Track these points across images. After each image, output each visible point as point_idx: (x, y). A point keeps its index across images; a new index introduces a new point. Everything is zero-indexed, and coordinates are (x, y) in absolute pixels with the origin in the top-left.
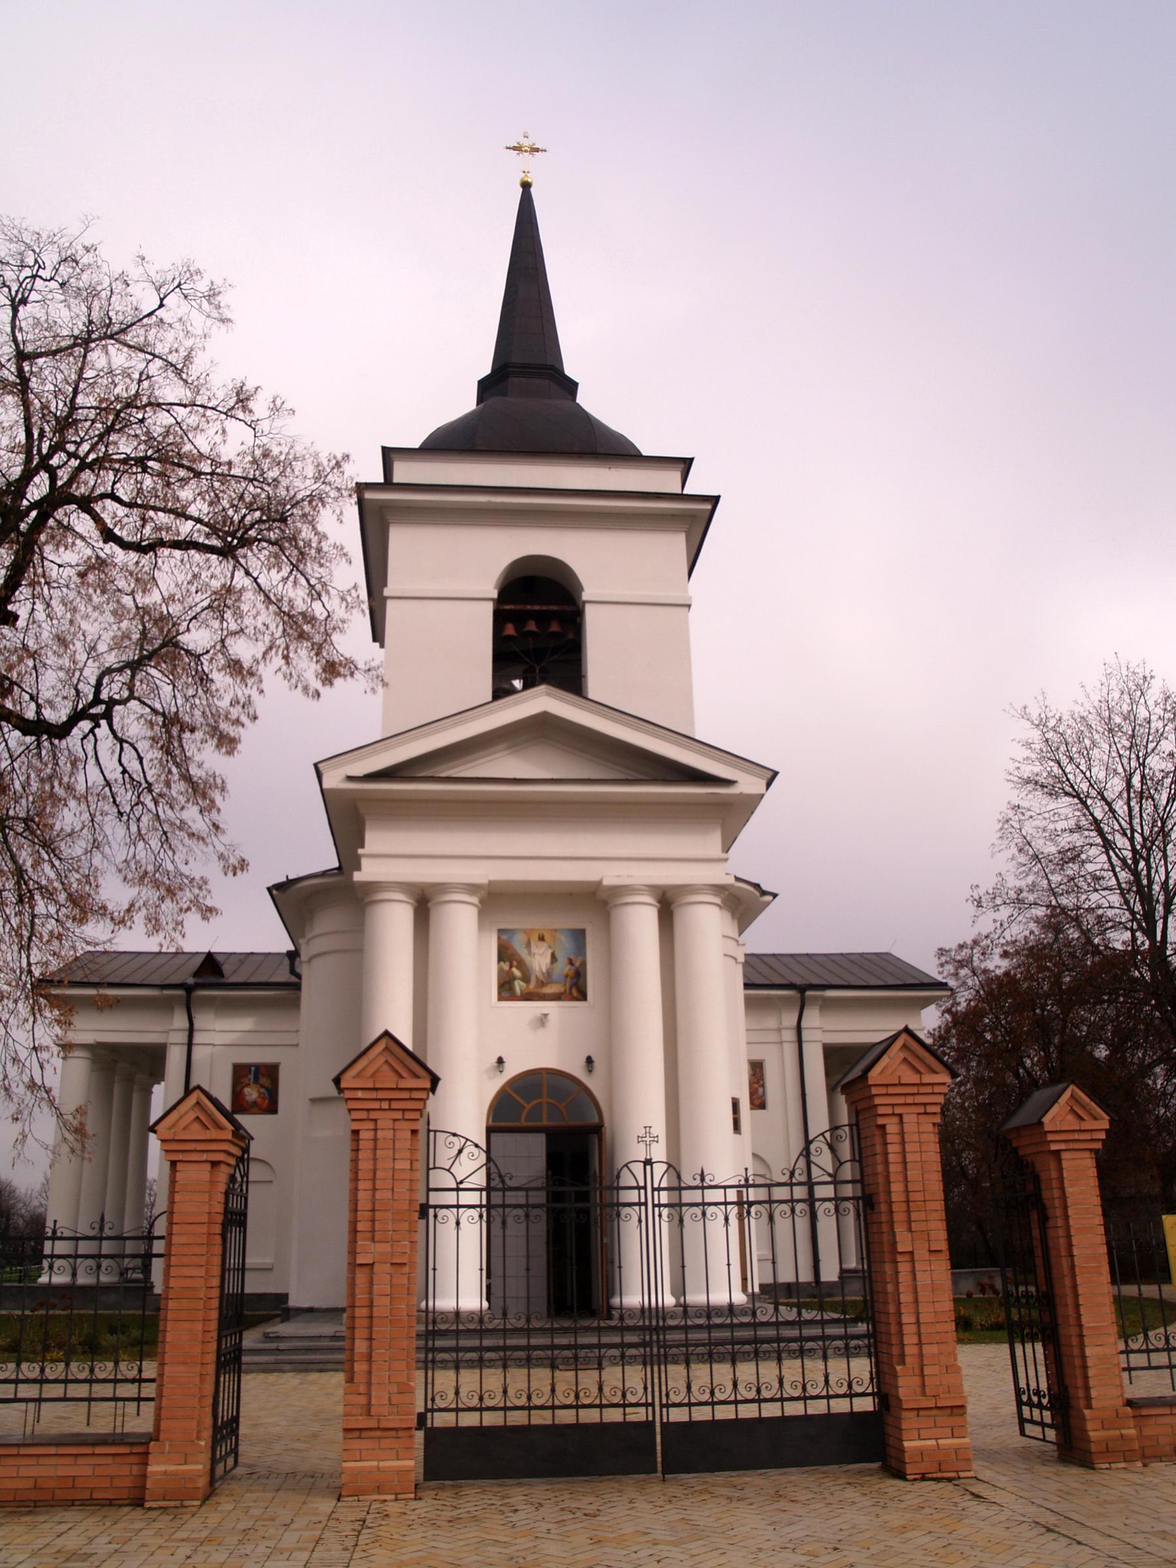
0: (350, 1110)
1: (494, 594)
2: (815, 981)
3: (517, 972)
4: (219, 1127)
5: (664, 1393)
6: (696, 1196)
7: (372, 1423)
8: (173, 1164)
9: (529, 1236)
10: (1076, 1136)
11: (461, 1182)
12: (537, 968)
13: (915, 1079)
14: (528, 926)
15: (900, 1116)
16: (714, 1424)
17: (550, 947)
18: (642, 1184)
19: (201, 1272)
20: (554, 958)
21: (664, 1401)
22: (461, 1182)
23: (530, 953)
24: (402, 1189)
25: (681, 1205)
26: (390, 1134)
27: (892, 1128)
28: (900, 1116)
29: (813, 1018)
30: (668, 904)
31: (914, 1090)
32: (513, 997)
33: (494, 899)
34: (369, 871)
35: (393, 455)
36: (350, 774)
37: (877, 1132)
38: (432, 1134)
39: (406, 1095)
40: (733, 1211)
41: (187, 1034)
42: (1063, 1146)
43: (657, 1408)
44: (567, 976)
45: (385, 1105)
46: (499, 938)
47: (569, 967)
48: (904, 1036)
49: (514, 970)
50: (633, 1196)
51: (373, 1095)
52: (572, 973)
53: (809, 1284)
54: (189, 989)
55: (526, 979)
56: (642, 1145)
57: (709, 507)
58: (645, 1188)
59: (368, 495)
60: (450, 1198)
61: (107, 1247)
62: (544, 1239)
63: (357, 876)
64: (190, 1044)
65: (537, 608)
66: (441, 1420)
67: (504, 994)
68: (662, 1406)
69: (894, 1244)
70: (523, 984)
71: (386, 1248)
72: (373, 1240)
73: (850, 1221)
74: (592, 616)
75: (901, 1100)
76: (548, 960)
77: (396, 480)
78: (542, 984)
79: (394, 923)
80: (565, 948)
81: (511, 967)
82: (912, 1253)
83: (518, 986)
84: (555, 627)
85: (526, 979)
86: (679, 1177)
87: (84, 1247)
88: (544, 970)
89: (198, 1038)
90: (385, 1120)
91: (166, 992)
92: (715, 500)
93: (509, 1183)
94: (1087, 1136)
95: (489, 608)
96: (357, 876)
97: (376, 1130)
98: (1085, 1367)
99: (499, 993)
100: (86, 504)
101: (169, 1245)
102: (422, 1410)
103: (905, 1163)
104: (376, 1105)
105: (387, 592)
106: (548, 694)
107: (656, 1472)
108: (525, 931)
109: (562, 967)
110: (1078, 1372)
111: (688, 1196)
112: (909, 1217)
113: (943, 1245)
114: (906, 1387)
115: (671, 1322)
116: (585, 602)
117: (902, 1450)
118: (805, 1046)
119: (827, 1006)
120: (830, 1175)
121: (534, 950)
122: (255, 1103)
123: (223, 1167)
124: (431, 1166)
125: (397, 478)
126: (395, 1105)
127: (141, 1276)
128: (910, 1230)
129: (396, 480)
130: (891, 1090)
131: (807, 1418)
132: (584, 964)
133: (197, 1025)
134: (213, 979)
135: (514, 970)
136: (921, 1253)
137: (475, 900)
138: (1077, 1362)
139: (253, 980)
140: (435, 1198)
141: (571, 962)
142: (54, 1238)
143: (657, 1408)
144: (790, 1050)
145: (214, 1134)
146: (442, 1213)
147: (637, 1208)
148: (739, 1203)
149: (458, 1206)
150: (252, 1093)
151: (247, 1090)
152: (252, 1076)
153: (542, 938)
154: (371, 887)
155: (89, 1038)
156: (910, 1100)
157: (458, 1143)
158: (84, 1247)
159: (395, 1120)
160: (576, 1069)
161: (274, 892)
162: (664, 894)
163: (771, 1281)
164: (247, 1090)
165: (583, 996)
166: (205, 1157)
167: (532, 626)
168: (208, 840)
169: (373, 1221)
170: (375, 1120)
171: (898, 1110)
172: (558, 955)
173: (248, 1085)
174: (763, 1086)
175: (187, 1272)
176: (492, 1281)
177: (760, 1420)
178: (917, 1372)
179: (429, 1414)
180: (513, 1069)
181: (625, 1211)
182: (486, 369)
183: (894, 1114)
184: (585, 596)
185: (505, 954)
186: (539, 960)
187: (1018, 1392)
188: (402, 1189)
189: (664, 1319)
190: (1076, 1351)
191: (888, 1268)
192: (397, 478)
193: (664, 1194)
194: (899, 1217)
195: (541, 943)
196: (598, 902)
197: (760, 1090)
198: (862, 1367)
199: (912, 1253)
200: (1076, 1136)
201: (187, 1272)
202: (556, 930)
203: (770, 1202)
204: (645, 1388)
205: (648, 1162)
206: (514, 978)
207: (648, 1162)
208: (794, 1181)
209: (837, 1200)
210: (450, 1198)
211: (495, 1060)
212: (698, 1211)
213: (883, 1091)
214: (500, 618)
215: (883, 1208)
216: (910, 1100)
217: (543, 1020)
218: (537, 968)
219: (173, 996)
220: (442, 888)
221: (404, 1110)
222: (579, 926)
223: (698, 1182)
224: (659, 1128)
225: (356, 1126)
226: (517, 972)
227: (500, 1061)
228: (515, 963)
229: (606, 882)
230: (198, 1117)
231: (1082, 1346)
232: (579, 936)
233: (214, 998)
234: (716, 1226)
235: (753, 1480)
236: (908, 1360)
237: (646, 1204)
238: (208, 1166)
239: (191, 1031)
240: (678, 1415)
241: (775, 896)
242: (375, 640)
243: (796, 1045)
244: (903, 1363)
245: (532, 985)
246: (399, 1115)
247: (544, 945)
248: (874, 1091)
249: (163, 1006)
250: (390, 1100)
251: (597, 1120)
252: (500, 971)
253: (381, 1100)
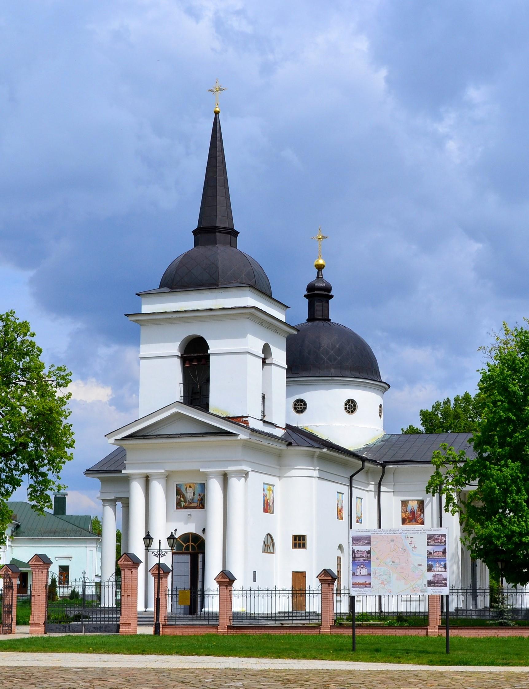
3: (182, 499)
14: (187, 482)
32: (181, 508)
55: (185, 502)
61: (244, 592)
65: (195, 355)
74: (213, 360)
78: (190, 503)
80: (198, 490)
83: (183, 504)
85: (185, 502)
109: (197, 497)
121: (188, 491)
132: (204, 496)
141: (200, 495)
153: (190, 487)
160: (200, 533)
184: (209, 352)
206: (181, 501)
222: (203, 482)
226: (182, 499)
247: (191, 489)
252: (177, 499)
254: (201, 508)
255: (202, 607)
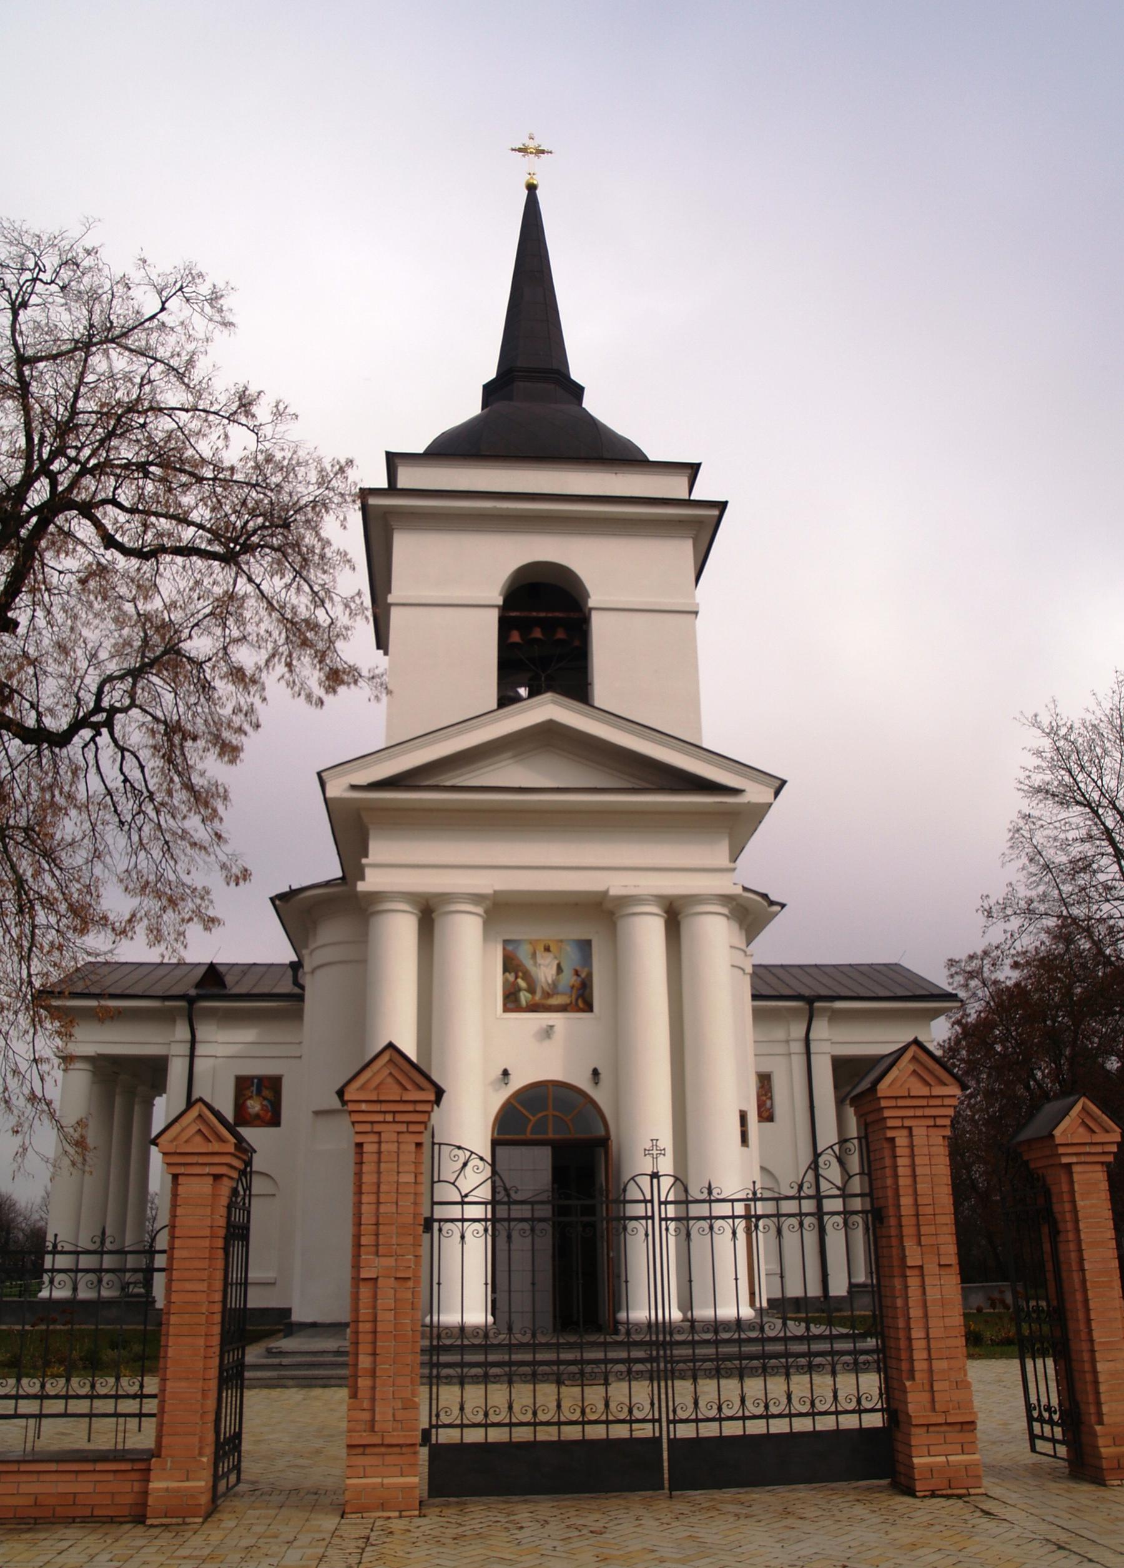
0: (353, 1123)
1: (500, 601)
2: (824, 992)
3: (522, 984)
4: (222, 1140)
5: (671, 1409)
6: (702, 1210)
7: (376, 1440)
8: (175, 1177)
9: (534, 1250)
10: (1088, 1149)
11: (466, 1196)
12: (543, 980)
13: (925, 1091)
14: (534, 937)
15: (910, 1128)
16: (721, 1440)
17: (556, 958)
18: (648, 1197)
19: (203, 1286)
20: (560, 969)
21: (671, 1417)
22: (466, 1196)
23: (535, 964)
24: (406, 1202)
25: (688, 1218)
26: (393, 1147)
27: (901, 1140)
28: (910, 1128)
29: (821, 1030)
30: (675, 915)
31: (924, 1102)
32: (519, 1009)
33: (499, 910)
34: (372, 881)
35: (397, 461)
36: (354, 783)
37: (886, 1145)
38: (436, 1147)
39: (410, 1107)
40: (741, 1225)
41: (188, 1045)
42: (1074, 1159)
43: (664, 1424)
44: (572, 987)
45: (389, 1118)
46: (504, 949)
47: (575, 978)
48: (913, 1048)
49: (520, 981)
50: (640, 1210)
51: (377, 1107)
52: (578, 984)
53: (818, 1298)
54: (191, 1000)
55: (531, 990)
56: (649, 1158)
57: (716, 512)
58: (652, 1201)
59: (372, 501)
60: (455, 1212)
61: (108, 1261)
62: (550, 1252)
63: (361, 886)
64: (192, 1056)
65: (542, 615)
66: (446, 1436)
67: (510, 1006)
68: (669, 1422)
69: (903, 1258)
70: (529, 995)
71: (391, 1262)
72: (377, 1254)
73: (859, 1235)
74: (598, 622)
75: (911, 1113)
76: (554, 971)
77: (400, 486)
78: (547, 995)
79: (399, 933)
80: (571, 959)
81: (516, 978)
82: (921, 1267)
83: (524, 997)
84: (561, 635)
85: (531, 990)
86: (686, 1191)
87: (85, 1261)
88: (550, 981)
89: (200, 1050)
90: (389, 1133)
91: (167, 1003)
92: (722, 506)
93: (515, 1196)
94: (1099, 1149)
95: (493, 616)
96: (361, 886)
97: (379, 1143)
98: (1096, 1382)
99: (505, 1005)
100: (87, 510)
101: (171, 1259)
102: (427, 1426)
103: (914, 1176)
104: (380, 1118)
105: (391, 599)
106: (554, 702)
107: (662, 1488)
108: (531, 942)
109: (568, 979)
110: (1090, 1388)
111: (695, 1210)
112: (919, 1230)
113: (953, 1260)
114: (916, 1403)
115: (678, 1337)
116: (591, 609)
117: (912, 1467)
118: (813, 1057)
119: (836, 1016)
120: (838, 1188)
121: (540, 961)
122: (257, 1116)
123: (226, 1181)
124: (436, 1179)
125: (402, 484)
126: (399, 1118)
127: (142, 1290)
128: (919, 1244)
129: (400, 486)
130: (901, 1103)
131: (815, 1434)
132: (590, 975)
133: (199, 1036)
134: (215, 991)
135: (520, 981)
136: (931, 1268)
137: (480, 910)
138: (1089, 1377)
139: (256, 991)
140: (440, 1212)
141: (577, 973)
142: (55, 1252)
143: (664, 1424)
144: (799, 1062)
145: (216, 1147)
146: (447, 1226)
147: (643, 1222)
148: (747, 1217)
149: (463, 1220)
150: (254, 1106)
151: (249, 1103)
152: (254, 1088)
153: (547, 949)
154: (375, 897)
155: (90, 1050)
156: (919, 1112)
157: (463, 1156)
158: (85, 1261)
159: (398, 1133)
160: (582, 1082)
161: (277, 902)
162: (671, 904)
163: (779, 1295)
164: (249, 1103)
165: (589, 1007)
166: (207, 1170)
167: (537, 633)
168: (211, 850)
169: (377, 1235)
170: (379, 1133)
171: (907, 1123)
172: (563, 965)
173: (250, 1098)
174: (771, 1098)
175: (189, 1286)
176: (497, 1296)
177: (768, 1437)
178: (927, 1387)
179: (434, 1431)
180: (518, 1082)
181: (631, 1224)
182: (491, 374)
183: (903, 1127)
184: (591, 603)
185: (510, 964)
186: (545, 971)
187: (1029, 1408)
188: (406, 1202)
189: (671, 1335)
190: (1087, 1367)
191: (897, 1283)
192: (402, 484)
193: (671, 1208)
194: (908, 1230)
195: (547, 954)
196: (605, 912)
197: (768, 1103)
198: (871, 1383)
199: (921, 1267)
200: (1088, 1149)
201: (189, 1286)
202: (561, 941)
203: (778, 1215)
204: (652, 1404)
205: (655, 1175)
206: (520, 990)
207: (655, 1175)
208: (802, 1194)
209: (846, 1213)
210: (455, 1212)
211: (500, 1072)
212: (705, 1224)
213: (892, 1103)
214: (505, 625)
215: (893, 1221)
216: (919, 1112)
217: (548, 1032)
218: (543, 980)
219: (176, 1008)
220: (446, 898)
221: (408, 1123)
223: (705, 1196)
224: (666, 1141)
225: (359, 1139)
226: (522, 984)
227: (506, 1073)
228: (520, 974)
229: (612, 892)
230: (200, 1130)
231: (1093, 1361)
232: (585, 946)
233: (217, 1009)
234: (723, 1241)
235: (761, 1497)
236: (917, 1375)
237: (652, 1218)
238: (210, 1180)
239: (193, 1042)
240: (685, 1431)
241: (783, 906)
242: (379, 647)
243: (804, 1057)
244: (912, 1378)
245: (538, 997)
246: (403, 1128)
248: (883, 1103)
249: (165, 1017)
250: (394, 1112)
251: (603, 1133)
252: (505, 982)
253: (385, 1112)
254: (583, 1011)
255: (617, 1308)
